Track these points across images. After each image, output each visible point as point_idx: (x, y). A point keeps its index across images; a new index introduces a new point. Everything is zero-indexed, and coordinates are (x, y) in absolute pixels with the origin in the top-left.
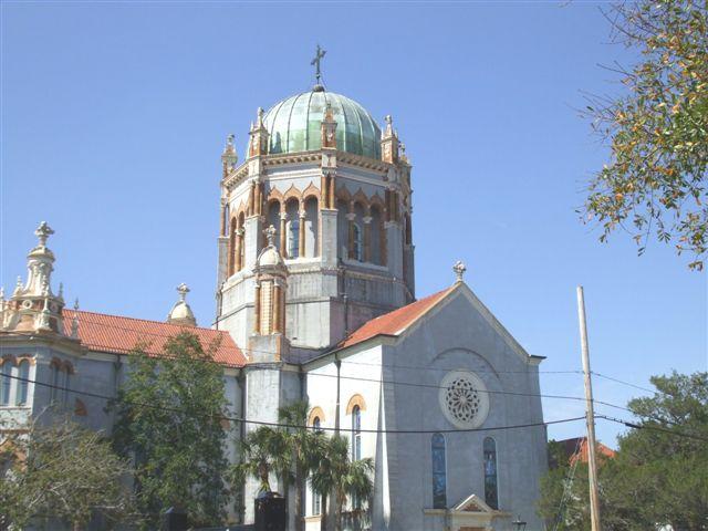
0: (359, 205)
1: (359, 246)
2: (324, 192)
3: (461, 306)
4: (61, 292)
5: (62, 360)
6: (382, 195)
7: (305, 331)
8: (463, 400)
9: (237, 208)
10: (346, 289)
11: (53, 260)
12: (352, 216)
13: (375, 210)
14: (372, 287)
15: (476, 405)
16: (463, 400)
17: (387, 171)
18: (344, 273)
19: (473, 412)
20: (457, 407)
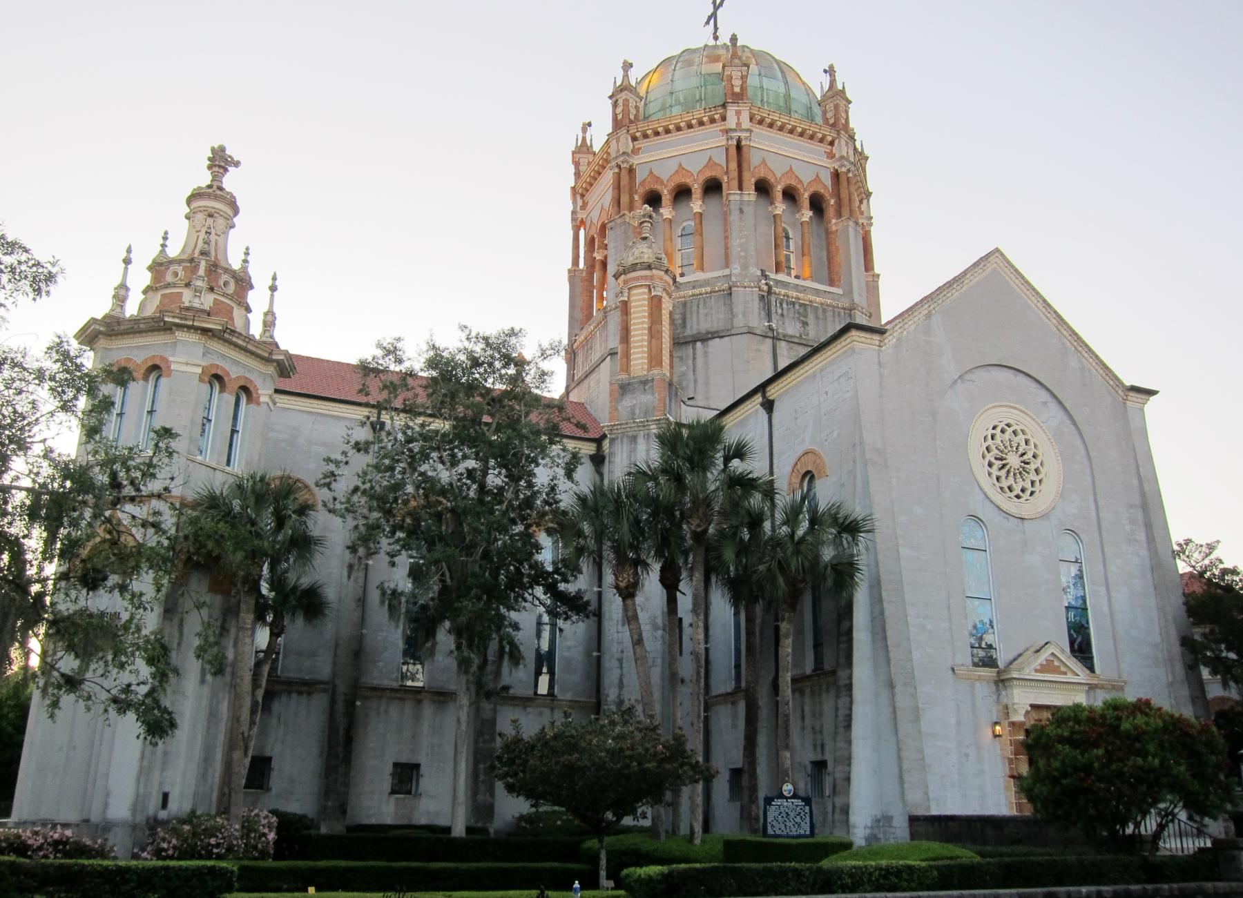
0: (790, 195)
1: (792, 257)
2: (733, 165)
3: (990, 288)
4: (245, 261)
5: (233, 376)
6: (828, 182)
7: (707, 384)
8: (1014, 461)
9: (595, 221)
10: (774, 316)
11: (236, 211)
12: (780, 207)
13: (817, 204)
14: (817, 318)
15: (1037, 471)
16: (1013, 466)
17: (832, 143)
18: (770, 292)
19: (1033, 483)
20: (1003, 472)
